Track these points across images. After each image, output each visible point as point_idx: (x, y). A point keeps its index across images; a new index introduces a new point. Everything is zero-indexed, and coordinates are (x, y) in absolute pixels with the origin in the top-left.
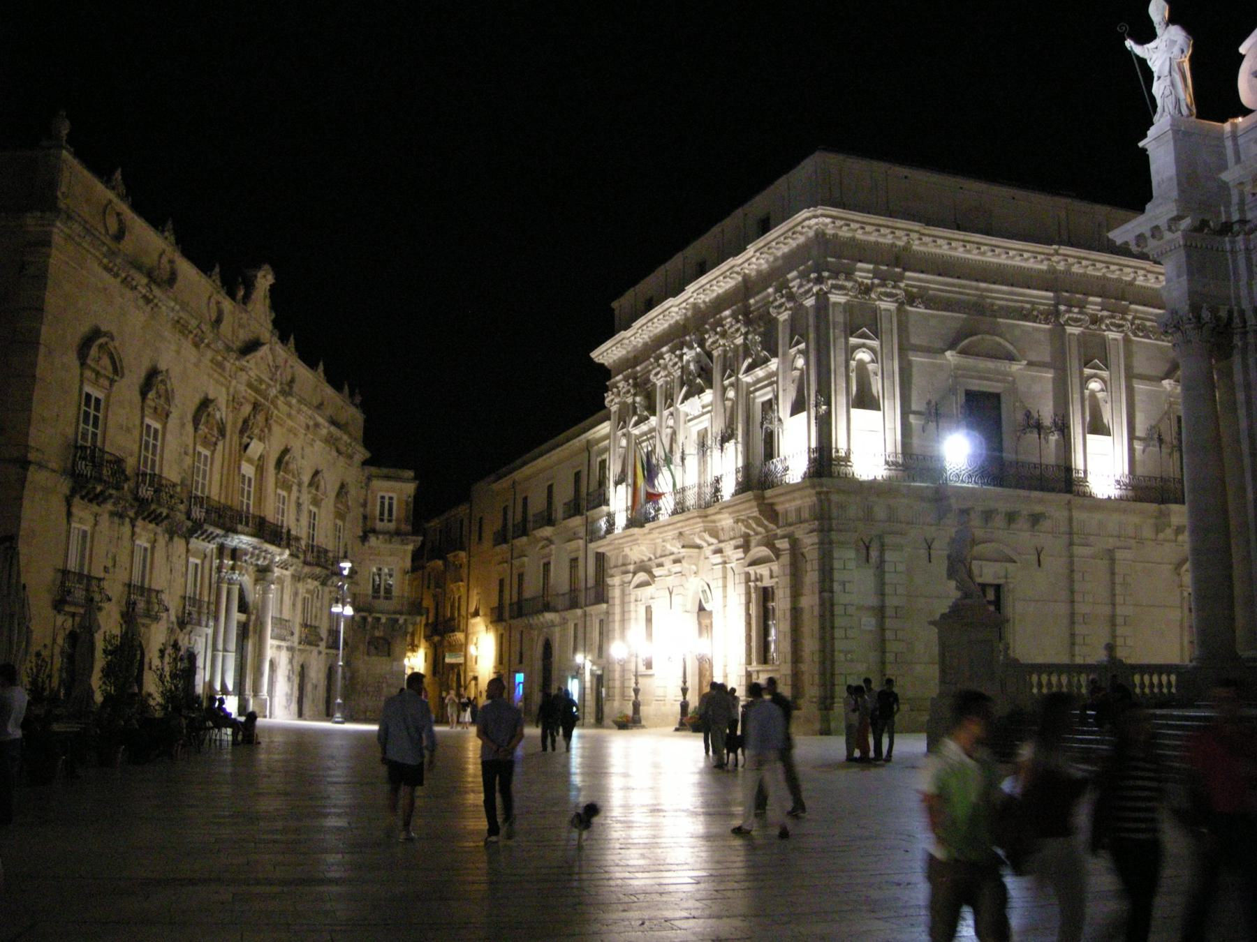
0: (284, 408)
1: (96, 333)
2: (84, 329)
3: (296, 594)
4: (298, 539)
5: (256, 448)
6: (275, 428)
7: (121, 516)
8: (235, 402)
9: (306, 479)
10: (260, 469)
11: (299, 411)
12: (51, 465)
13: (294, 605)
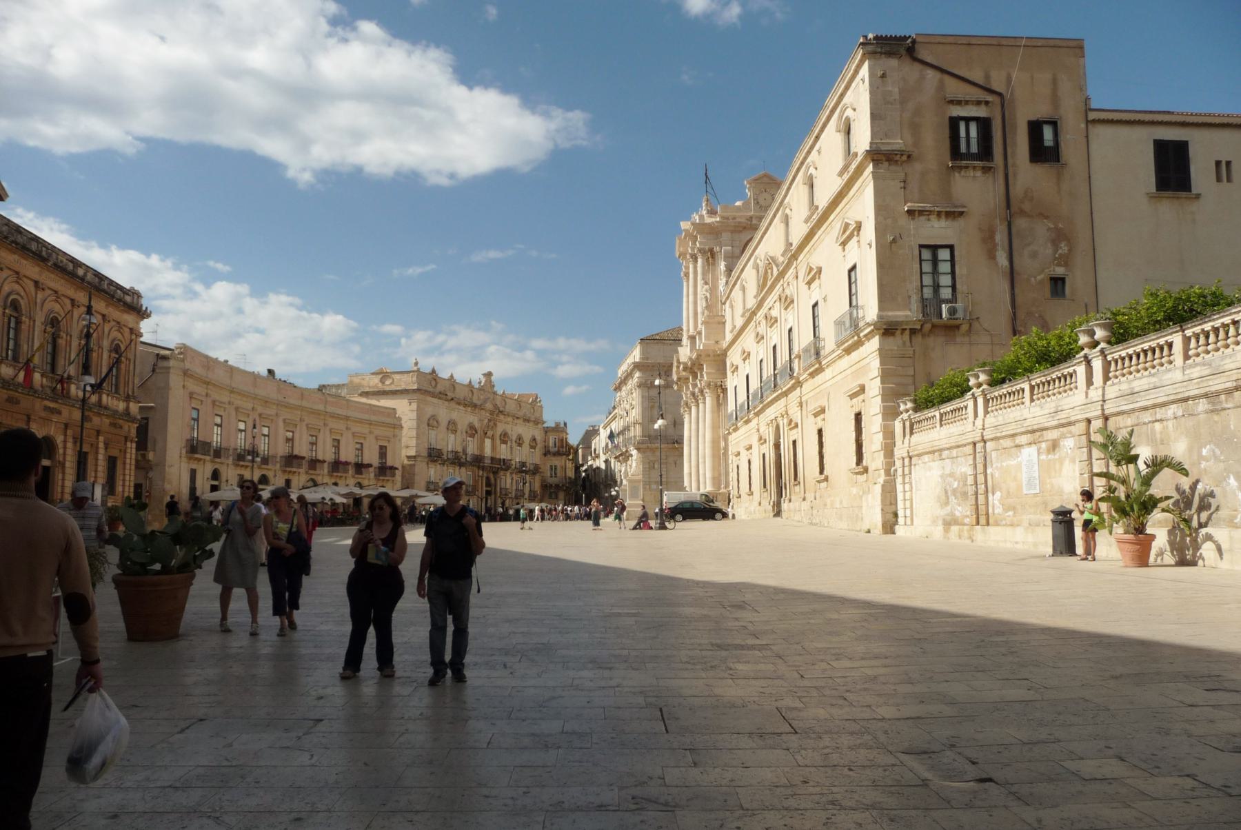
0: (502, 417)
1: (433, 416)
2: (428, 416)
3: (512, 479)
5: (490, 433)
6: (498, 424)
7: (444, 464)
8: (481, 420)
9: (514, 438)
10: (493, 438)
13: (512, 483)
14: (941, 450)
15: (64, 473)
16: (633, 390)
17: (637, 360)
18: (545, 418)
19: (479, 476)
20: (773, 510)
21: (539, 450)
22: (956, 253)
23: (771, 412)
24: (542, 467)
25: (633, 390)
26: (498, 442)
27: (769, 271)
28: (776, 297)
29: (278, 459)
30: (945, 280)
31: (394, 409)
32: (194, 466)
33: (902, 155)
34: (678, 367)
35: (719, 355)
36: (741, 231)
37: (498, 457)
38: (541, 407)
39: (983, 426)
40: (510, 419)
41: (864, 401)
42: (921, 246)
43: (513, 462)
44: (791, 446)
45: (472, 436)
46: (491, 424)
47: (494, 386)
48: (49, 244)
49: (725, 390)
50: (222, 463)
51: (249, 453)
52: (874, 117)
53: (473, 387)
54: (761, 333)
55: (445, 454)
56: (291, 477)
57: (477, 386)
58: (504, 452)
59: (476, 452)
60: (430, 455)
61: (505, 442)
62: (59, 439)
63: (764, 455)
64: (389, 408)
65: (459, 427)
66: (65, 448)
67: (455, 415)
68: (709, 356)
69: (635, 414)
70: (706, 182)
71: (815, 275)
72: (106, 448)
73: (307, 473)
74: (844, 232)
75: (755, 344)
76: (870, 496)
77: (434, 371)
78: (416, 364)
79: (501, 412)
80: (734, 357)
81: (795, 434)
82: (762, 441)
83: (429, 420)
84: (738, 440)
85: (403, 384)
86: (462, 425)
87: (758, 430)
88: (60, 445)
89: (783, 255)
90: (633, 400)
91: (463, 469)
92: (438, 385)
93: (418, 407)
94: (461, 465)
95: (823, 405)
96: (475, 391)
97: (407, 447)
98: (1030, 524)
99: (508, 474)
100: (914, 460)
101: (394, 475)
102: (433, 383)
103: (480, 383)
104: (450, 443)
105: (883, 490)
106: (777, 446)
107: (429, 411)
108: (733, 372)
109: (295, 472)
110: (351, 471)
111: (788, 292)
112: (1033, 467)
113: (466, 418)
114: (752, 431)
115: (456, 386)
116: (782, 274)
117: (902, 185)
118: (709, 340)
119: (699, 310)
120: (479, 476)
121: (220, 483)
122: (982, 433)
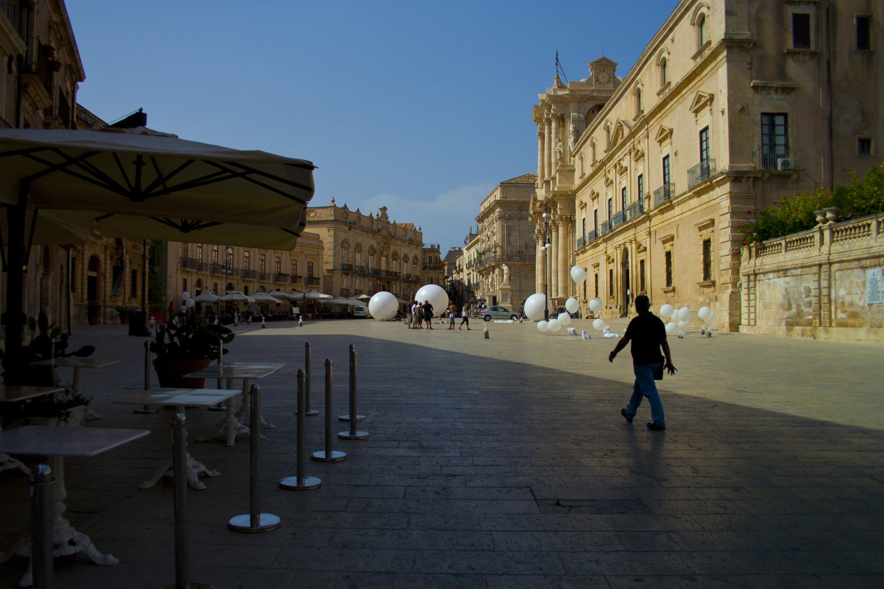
0: (393, 240)
1: (345, 240)
2: (342, 240)
3: (401, 287)
4: (400, 273)
5: (385, 253)
6: (391, 246)
7: (353, 276)
8: (379, 244)
9: (402, 257)
10: (387, 257)
11: (398, 240)
12: (338, 269)
13: (400, 290)
14: (787, 270)
15: (105, 282)
16: (494, 221)
17: (498, 198)
18: (424, 241)
19: (377, 284)
20: (620, 312)
21: (419, 267)
22: (789, 120)
23: (619, 240)
24: (421, 278)
25: (494, 221)
26: (391, 259)
27: (621, 132)
28: (627, 150)
29: (240, 272)
30: (780, 140)
31: (318, 235)
32: (185, 277)
33: (749, 43)
34: (534, 204)
35: (569, 195)
36: (585, 102)
37: (391, 270)
38: (421, 233)
39: (829, 251)
40: (399, 242)
41: (713, 231)
42: (763, 114)
43: (401, 275)
44: (639, 265)
45: (373, 255)
46: (386, 246)
47: (388, 218)
48: (93, 115)
49: (573, 222)
50: (203, 275)
51: (223, 267)
52: (728, 13)
53: (373, 218)
54: (611, 179)
55: (354, 268)
56: (248, 285)
57: (375, 217)
58: (394, 266)
59: (376, 267)
60: (343, 269)
61: (395, 260)
62: (102, 257)
63: (611, 271)
64: (315, 234)
65: (364, 248)
66: (105, 263)
67: (360, 239)
68: (562, 195)
69: (496, 239)
70: (557, 64)
71: (665, 135)
72: (130, 266)
73: (259, 282)
74: (698, 102)
75: (604, 187)
76: (718, 304)
77: (345, 207)
78: (333, 201)
79: (392, 237)
80: (584, 196)
81: (642, 256)
82: (609, 260)
83: (343, 242)
84: (584, 260)
85: (323, 216)
86: (366, 247)
87: (606, 252)
88: (103, 262)
89: (634, 120)
90: (494, 228)
91: (367, 280)
92: (349, 218)
93: (335, 233)
94: (365, 276)
95: (672, 234)
96: (374, 221)
97: (327, 263)
98: (872, 327)
99: (398, 283)
100: (759, 277)
101: (318, 284)
102: (345, 215)
103: (378, 215)
104: (359, 260)
105: (730, 299)
106: (625, 263)
107: (342, 236)
108: (582, 209)
109: (251, 281)
110: (289, 281)
111: (639, 147)
112: (877, 283)
113: (368, 241)
114: (602, 252)
115: (361, 217)
116: (633, 135)
117: (749, 66)
118: (561, 184)
119: (553, 161)
120: (377, 284)
121: (202, 288)
122: (829, 257)
